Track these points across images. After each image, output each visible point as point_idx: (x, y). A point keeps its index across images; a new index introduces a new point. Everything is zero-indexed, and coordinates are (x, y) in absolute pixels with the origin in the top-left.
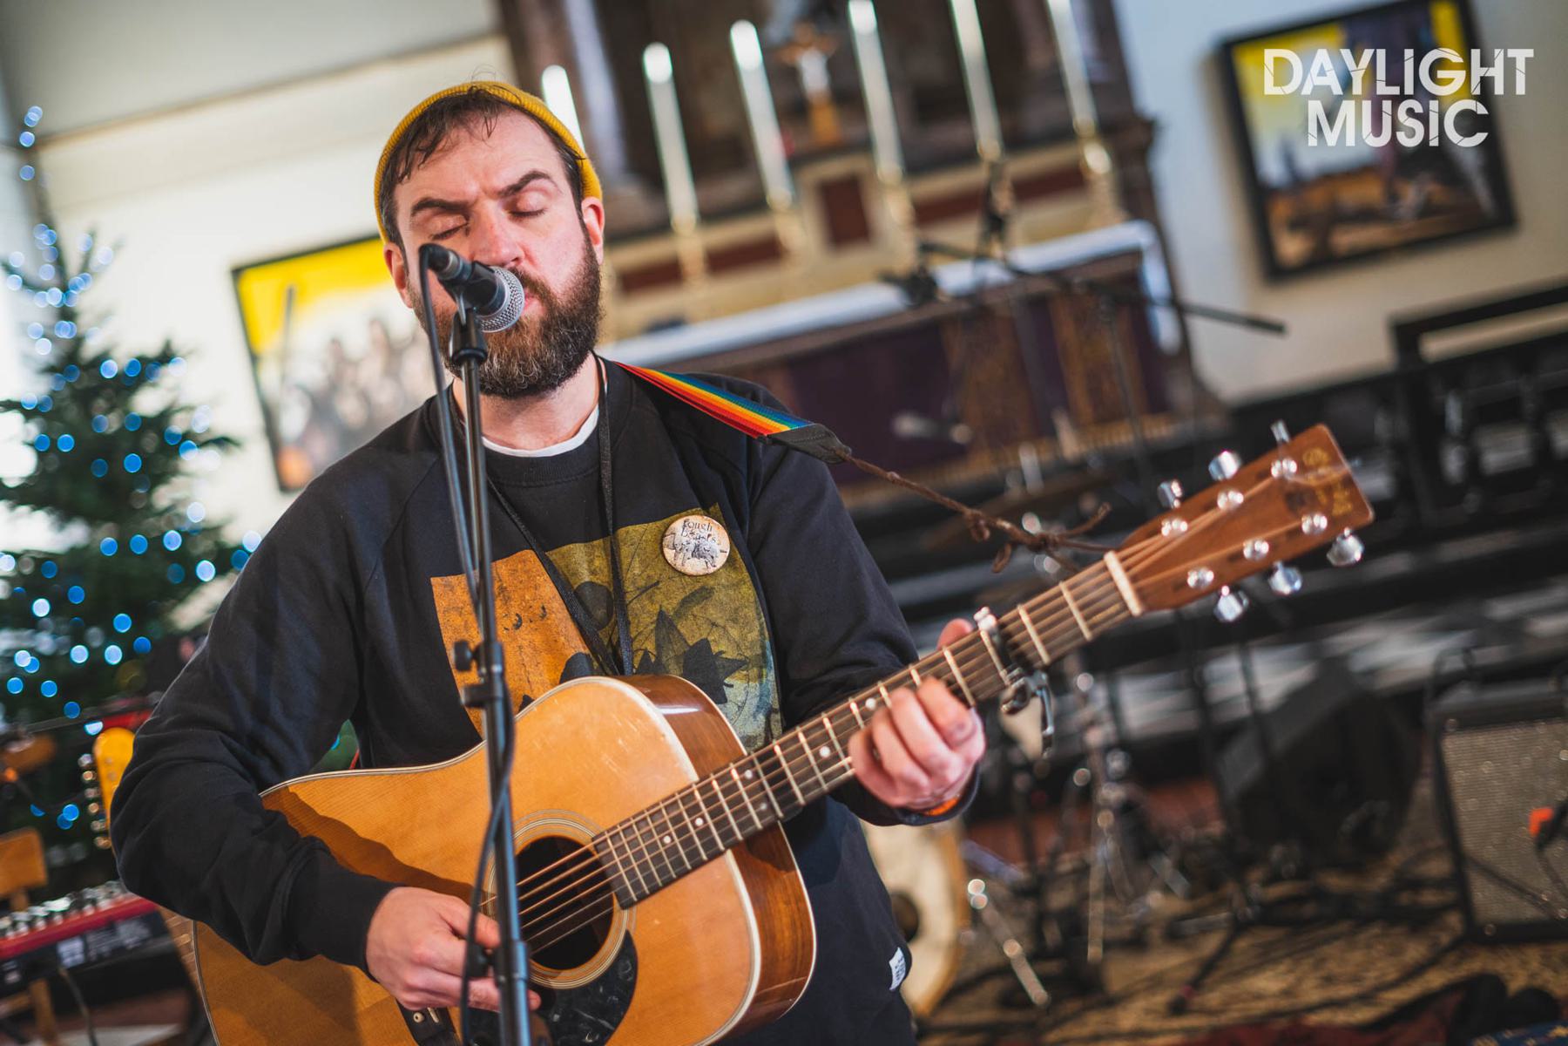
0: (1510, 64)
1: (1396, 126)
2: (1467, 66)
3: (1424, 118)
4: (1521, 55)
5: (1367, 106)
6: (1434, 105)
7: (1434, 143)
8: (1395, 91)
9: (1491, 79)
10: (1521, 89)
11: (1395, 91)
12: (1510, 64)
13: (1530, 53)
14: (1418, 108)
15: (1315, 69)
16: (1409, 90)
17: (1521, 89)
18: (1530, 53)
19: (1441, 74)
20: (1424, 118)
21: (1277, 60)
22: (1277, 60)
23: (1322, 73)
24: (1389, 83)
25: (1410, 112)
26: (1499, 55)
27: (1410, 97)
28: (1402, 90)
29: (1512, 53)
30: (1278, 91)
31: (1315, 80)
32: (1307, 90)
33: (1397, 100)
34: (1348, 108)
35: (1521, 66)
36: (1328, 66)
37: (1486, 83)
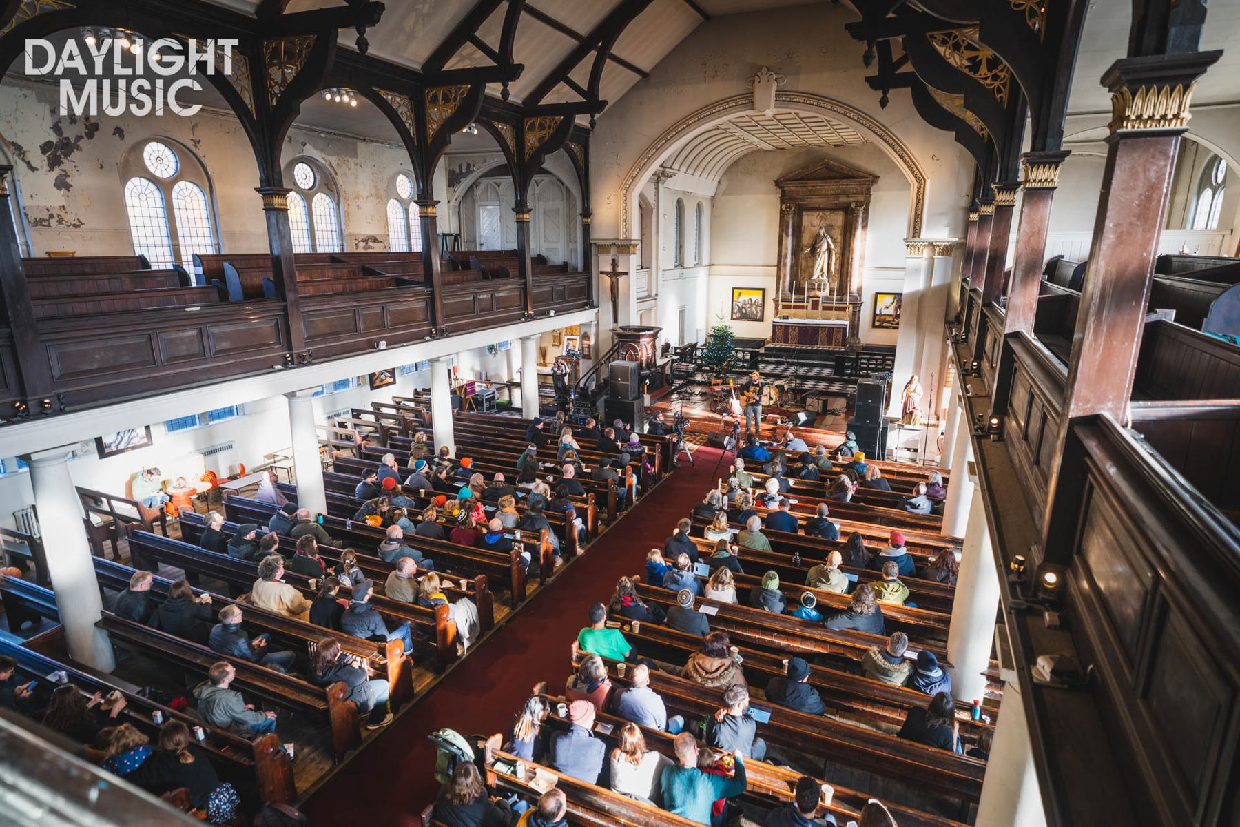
0: (220, 48)
1: (130, 99)
2: (184, 52)
3: (151, 93)
4: (229, 44)
5: (106, 83)
6: (159, 83)
7: (160, 113)
8: (129, 72)
9: (206, 62)
10: (228, 70)
11: (129, 72)
12: (220, 48)
13: (235, 42)
14: (147, 86)
15: (65, 55)
16: (140, 71)
17: (228, 70)
18: (235, 42)
19: (166, 59)
20: (151, 93)
21: (37, 49)
22: (34, 47)
23: (71, 57)
24: (124, 65)
25: (141, 89)
26: (211, 43)
27: (140, 77)
28: (134, 71)
29: (221, 42)
30: (36, 72)
31: (65, 63)
32: (59, 72)
33: (130, 80)
34: (91, 85)
35: (228, 52)
36: (76, 52)
37: (202, 65)
